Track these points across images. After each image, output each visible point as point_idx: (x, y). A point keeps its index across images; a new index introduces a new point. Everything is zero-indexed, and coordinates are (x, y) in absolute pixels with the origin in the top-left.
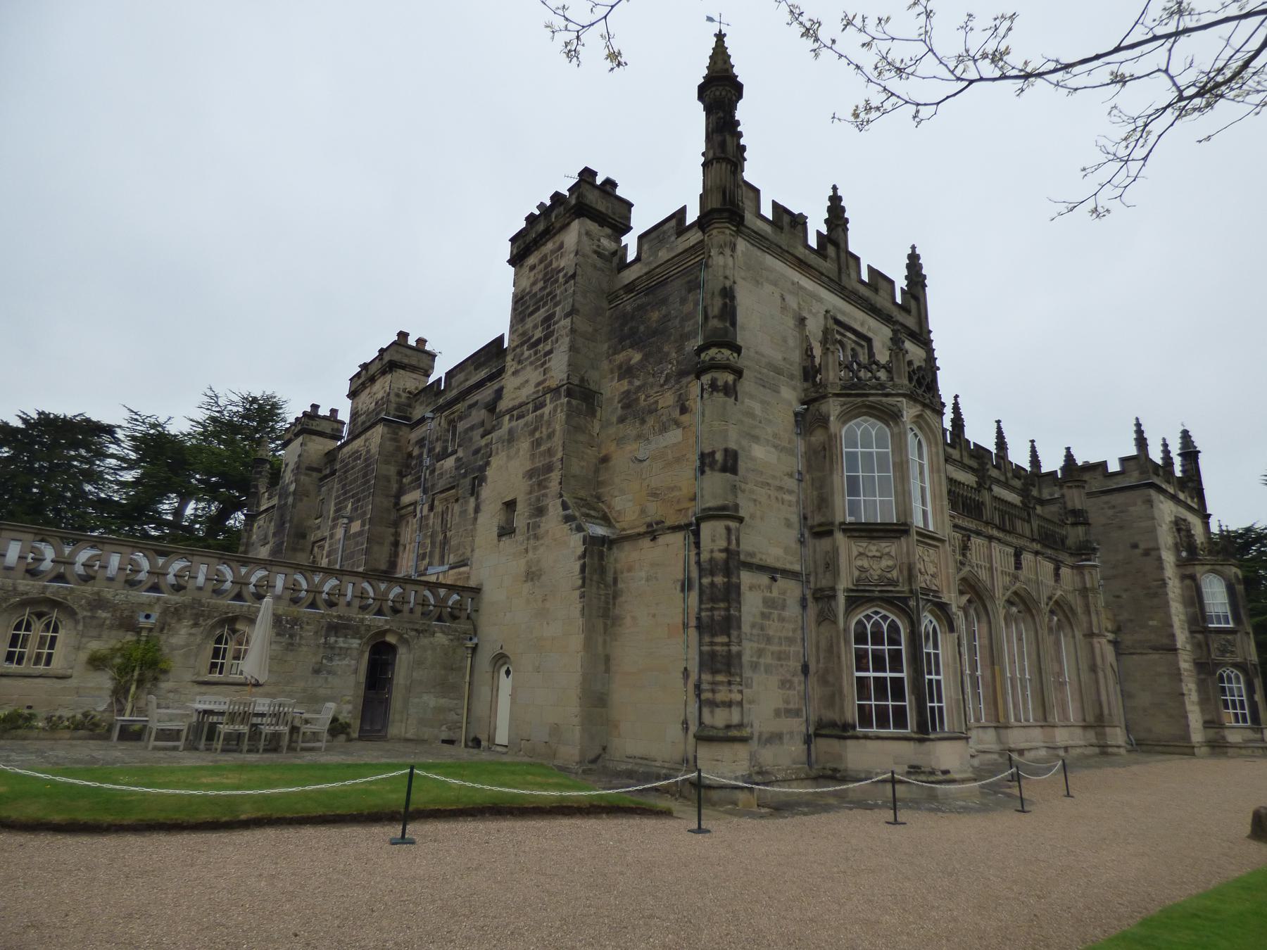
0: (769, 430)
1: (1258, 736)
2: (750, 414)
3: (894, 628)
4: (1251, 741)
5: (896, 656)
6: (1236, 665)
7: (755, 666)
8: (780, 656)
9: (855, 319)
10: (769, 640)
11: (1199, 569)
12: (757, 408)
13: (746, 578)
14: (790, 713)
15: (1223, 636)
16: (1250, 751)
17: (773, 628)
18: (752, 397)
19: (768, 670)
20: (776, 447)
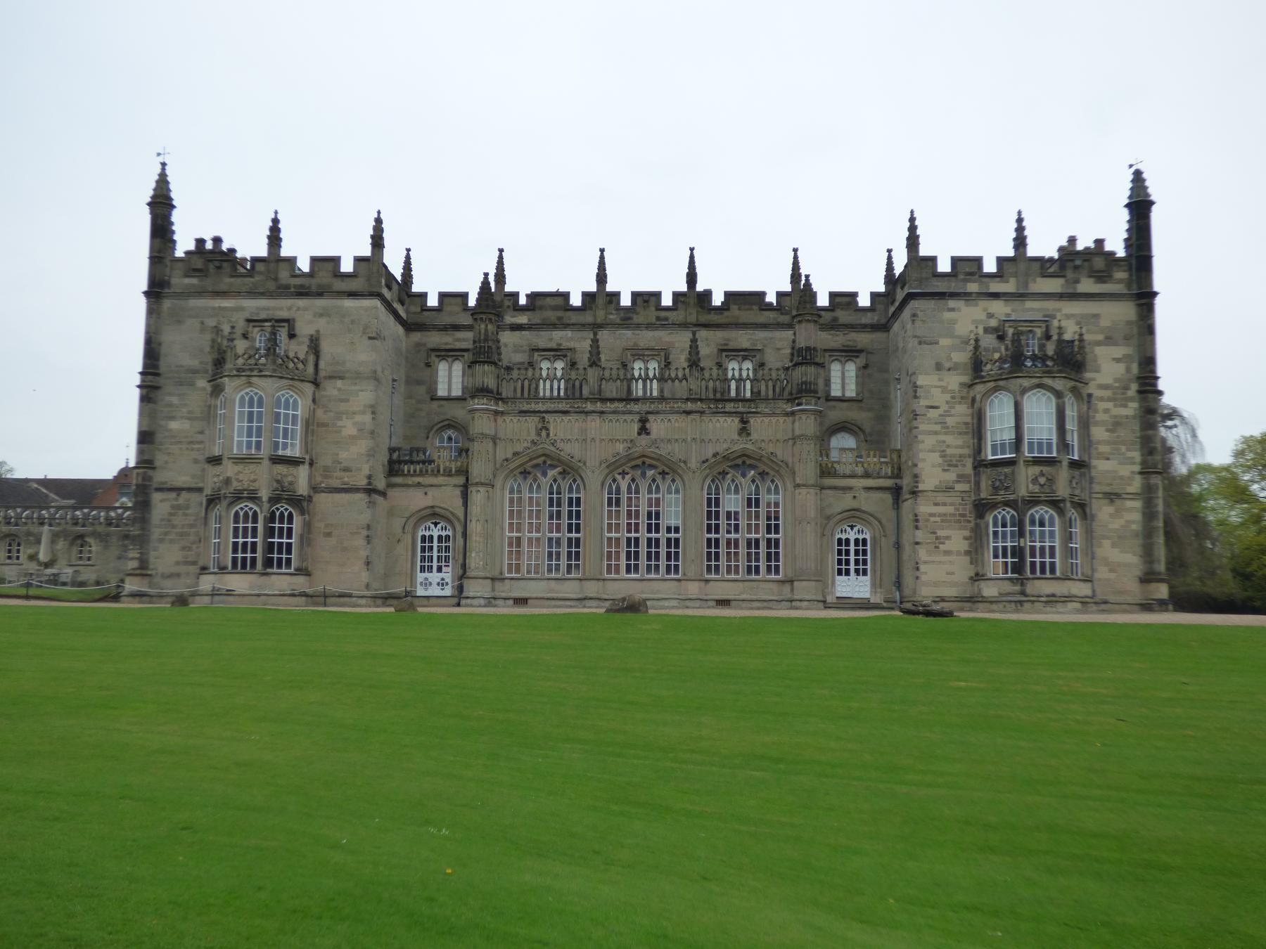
0: (184, 410)
1: (1018, 588)
2: (170, 405)
3: (255, 514)
4: (1008, 594)
5: (255, 530)
6: (1007, 504)
7: (161, 541)
8: (182, 534)
9: (281, 309)
10: (174, 527)
11: (980, 389)
12: (175, 400)
13: (156, 497)
14: (186, 563)
15: (999, 469)
16: (1001, 606)
17: (178, 520)
18: (170, 394)
19: (172, 541)
20: (189, 419)
